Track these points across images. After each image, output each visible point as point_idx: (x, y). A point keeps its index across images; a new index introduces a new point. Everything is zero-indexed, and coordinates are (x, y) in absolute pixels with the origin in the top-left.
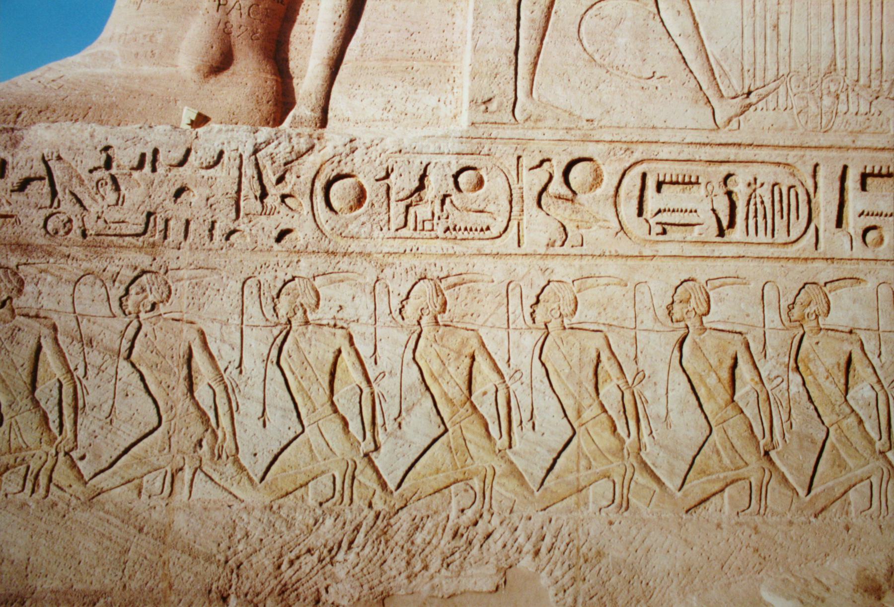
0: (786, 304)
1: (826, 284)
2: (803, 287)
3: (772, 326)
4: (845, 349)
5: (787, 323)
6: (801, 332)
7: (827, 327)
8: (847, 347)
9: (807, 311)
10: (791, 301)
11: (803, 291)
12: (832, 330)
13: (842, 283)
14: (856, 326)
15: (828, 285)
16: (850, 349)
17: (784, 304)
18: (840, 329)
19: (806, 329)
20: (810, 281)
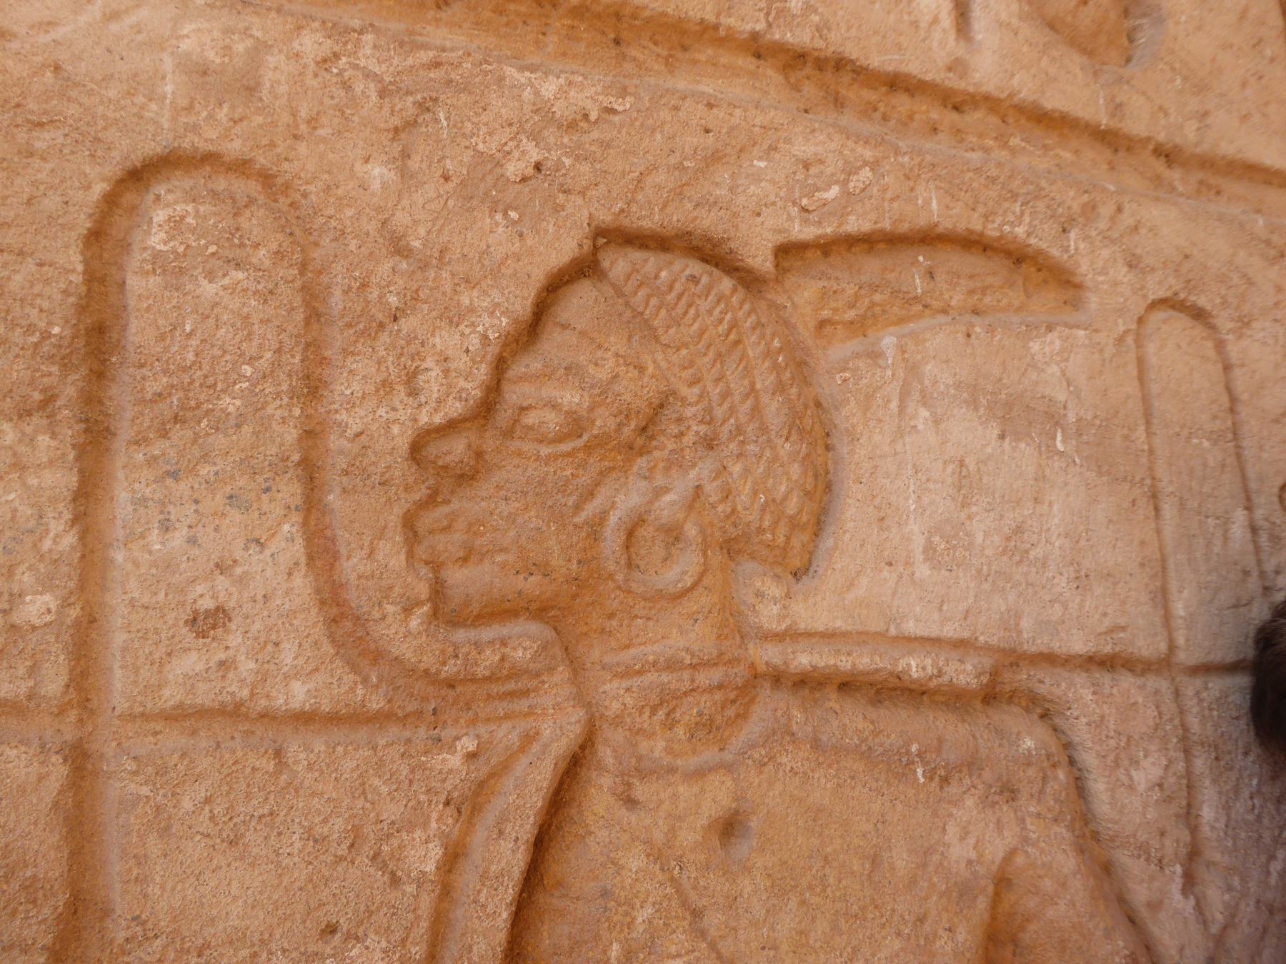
0: (399, 421)
1: (787, 252)
2: (583, 269)
3: (188, 671)
4: (959, 852)
5: (406, 635)
6: (558, 732)
7: (804, 660)
8: (973, 836)
9: (626, 498)
10: (450, 384)
11: (581, 302)
12: (847, 685)
13: (913, 272)
14: (1032, 638)
15: (804, 295)
16: (996, 849)
17: (371, 416)
18: (915, 666)
19: (615, 695)
20: (648, 219)
